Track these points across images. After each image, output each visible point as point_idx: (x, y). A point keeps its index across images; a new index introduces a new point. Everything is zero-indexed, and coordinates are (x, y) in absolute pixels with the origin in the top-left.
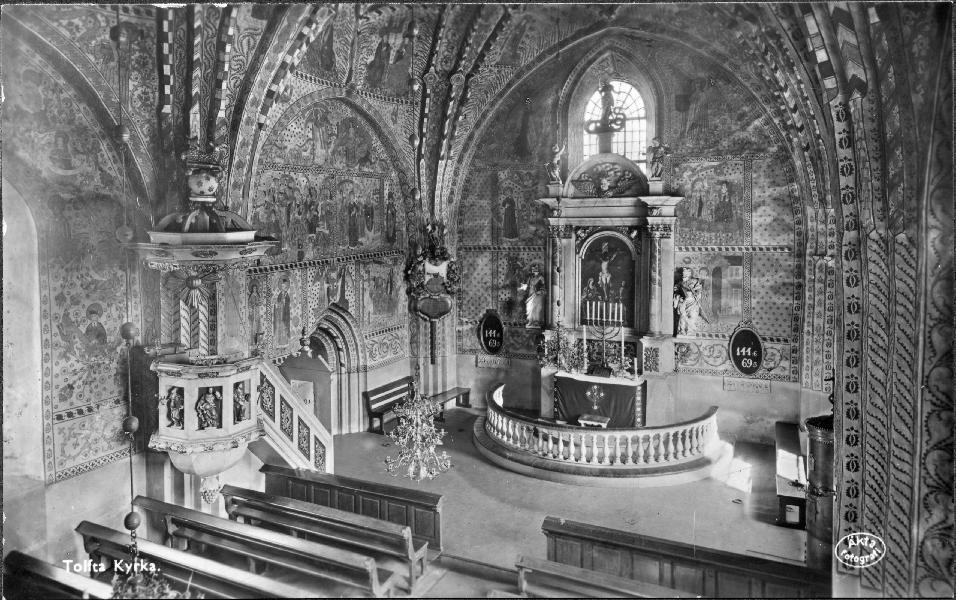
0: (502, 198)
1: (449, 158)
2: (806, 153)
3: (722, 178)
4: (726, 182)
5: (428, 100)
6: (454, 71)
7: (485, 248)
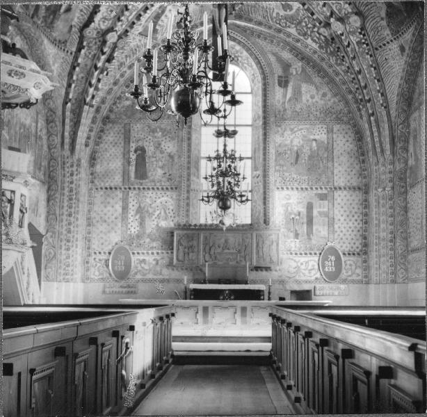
0: (133, 146)
1: (92, 106)
2: (372, 118)
3: (312, 137)
4: (315, 140)
5: (83, 51)
6: (111, 30)
7: (116, 188)
